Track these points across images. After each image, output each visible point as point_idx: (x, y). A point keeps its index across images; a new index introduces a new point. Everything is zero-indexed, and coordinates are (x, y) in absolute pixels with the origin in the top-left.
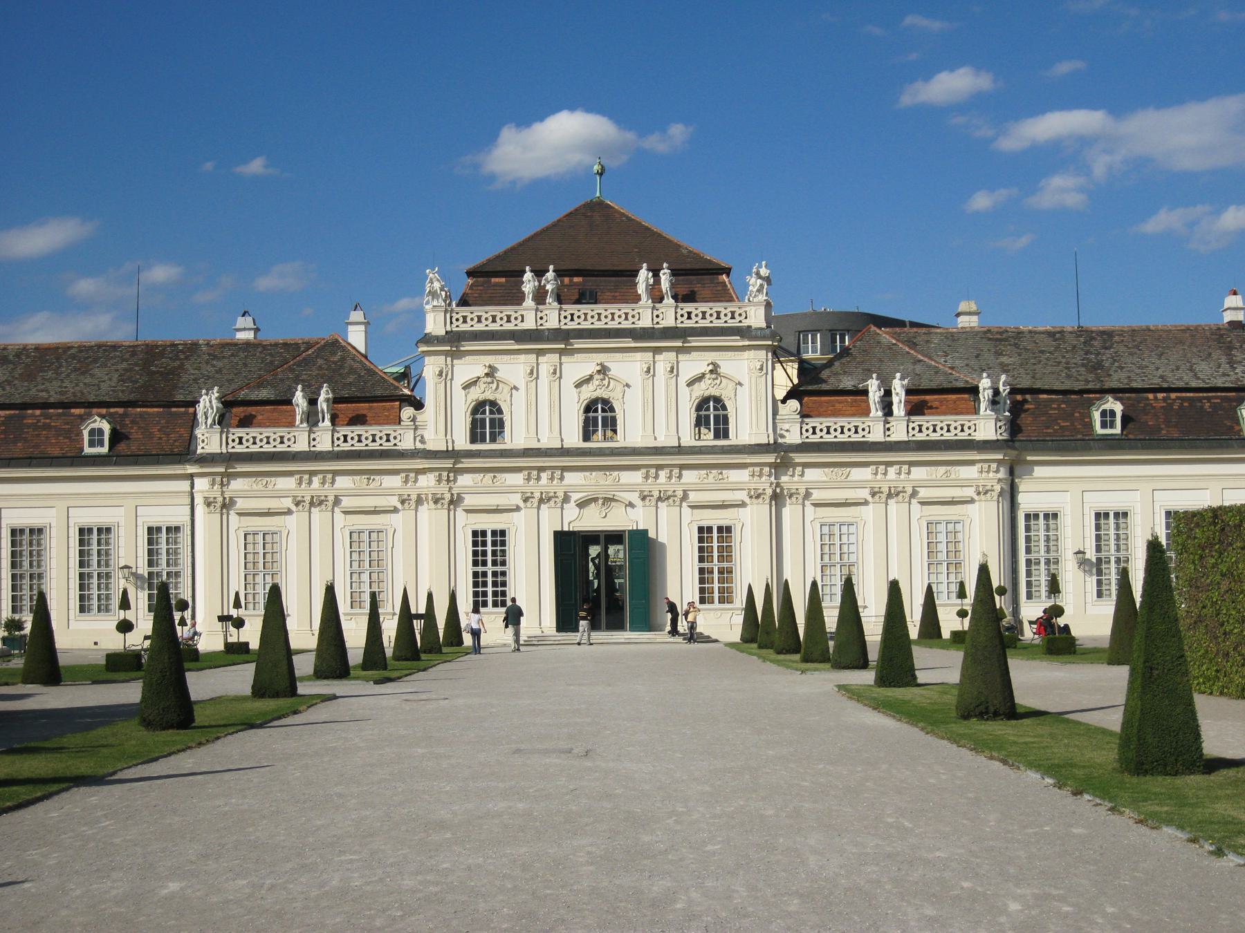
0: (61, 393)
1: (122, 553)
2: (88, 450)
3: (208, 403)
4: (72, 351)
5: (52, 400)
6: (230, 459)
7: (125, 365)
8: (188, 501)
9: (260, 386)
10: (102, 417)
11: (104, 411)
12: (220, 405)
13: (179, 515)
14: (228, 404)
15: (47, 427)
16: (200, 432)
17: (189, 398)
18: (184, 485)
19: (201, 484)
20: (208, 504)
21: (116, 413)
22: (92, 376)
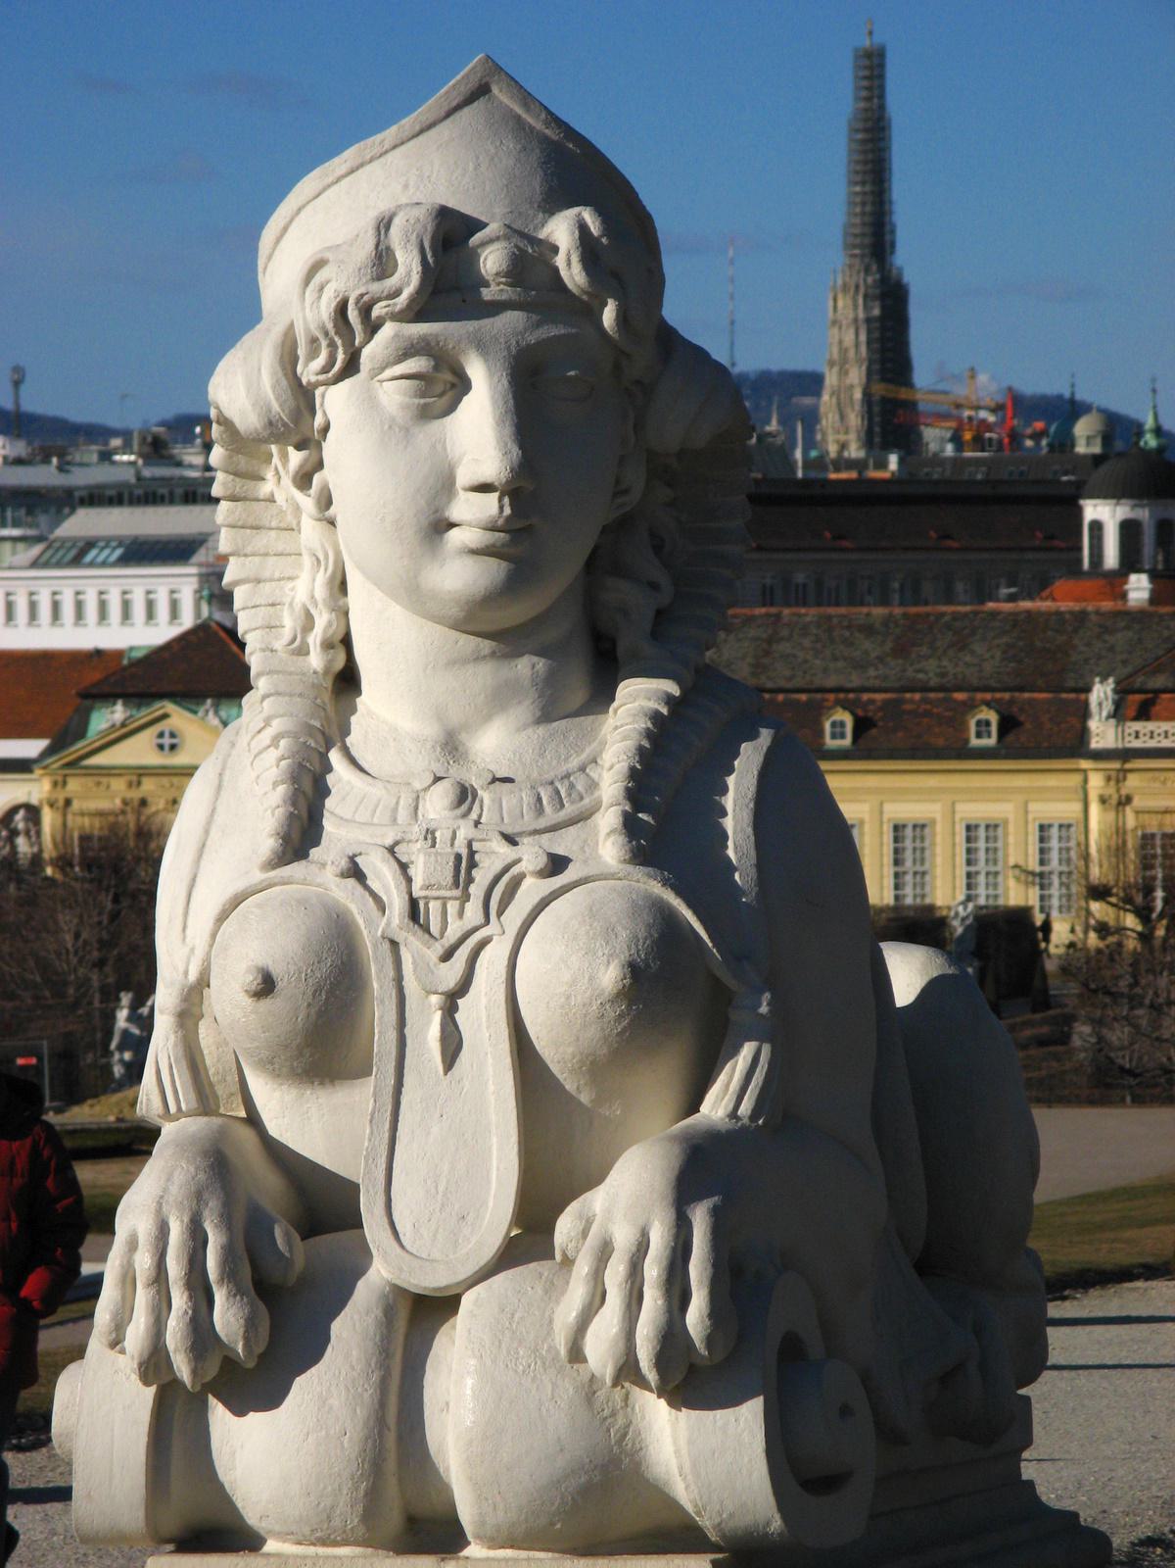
0: (943, 675)
1: (1011, 850)
2: (975, 742)
3: (1101, 694)
4: (947, 618)
5: (932, 683)
6: (1126, 755)
7: (1005, 639)
8: (1081, 795)
9: (1157, 671)
10: (988, 704)
11: (988, 696)
12: (1116, 697)
13: (1070, 810)
14: (1122, 692)
15: (927, 714)
16: (1093, 724)
17: (1081, 684)
18: (1077, 779)
19: (1096, 781)
20: (1103, 800)
21: (1001, 699)
22: (973, 652)
